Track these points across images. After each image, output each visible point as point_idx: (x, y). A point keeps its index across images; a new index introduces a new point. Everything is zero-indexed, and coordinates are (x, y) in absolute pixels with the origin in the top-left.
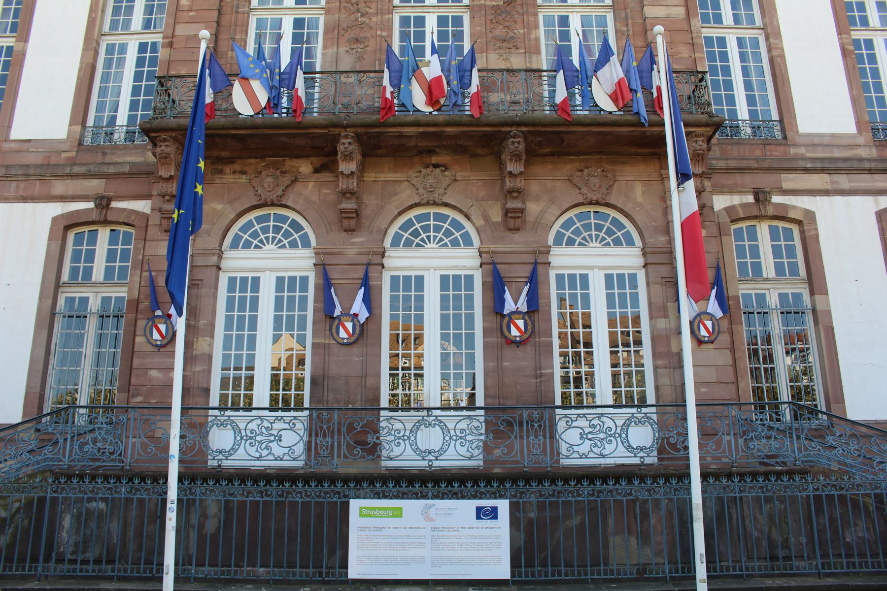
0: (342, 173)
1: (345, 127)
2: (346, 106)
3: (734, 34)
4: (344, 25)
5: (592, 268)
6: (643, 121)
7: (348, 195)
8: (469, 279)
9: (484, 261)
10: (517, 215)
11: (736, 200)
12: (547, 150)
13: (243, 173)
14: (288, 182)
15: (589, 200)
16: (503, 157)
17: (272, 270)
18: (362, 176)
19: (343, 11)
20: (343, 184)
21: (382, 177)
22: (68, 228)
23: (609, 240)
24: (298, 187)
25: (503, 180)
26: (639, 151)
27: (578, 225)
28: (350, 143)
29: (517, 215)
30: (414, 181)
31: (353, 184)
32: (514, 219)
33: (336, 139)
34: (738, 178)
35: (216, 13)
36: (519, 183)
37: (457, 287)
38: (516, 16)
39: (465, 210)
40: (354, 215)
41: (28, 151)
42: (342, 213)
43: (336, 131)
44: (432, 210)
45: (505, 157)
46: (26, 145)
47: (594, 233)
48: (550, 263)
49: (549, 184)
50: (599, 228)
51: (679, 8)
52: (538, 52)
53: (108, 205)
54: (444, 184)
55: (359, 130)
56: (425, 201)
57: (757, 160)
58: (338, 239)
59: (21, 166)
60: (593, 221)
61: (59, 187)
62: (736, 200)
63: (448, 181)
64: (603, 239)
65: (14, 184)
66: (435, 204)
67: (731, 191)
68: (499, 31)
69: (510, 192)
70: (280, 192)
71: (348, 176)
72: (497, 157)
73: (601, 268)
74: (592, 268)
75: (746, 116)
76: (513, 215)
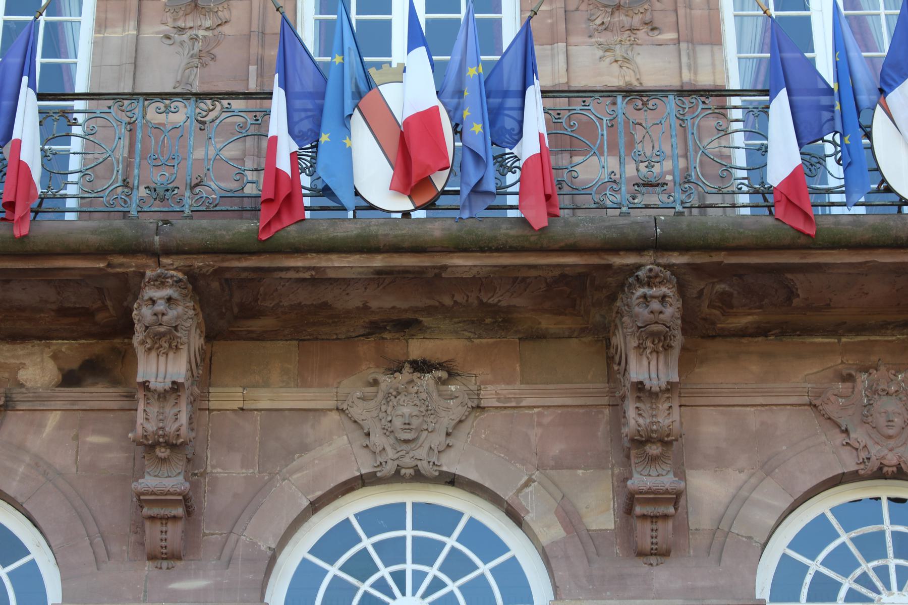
0: (145, 385)
1: (156, 254)
2: (160, 194)
7: (162, 452)
10: (661, 510)
12: (743, 321)
15: (874, 465)
16: (618, 340)
18: (205, 397)
20: (147, 419)
21: (265, 400)
25: (617, 407)
27: (844, 538)
28: (169, 300)
29: (661, 510)
30: (358, 411)
31: (177, 419)
32: (652, 525)
33: (128, 288)
36: (666, 417)
39: (507, 495)
43: (131, 264)
44: (409, 497)
45: (624, 340)
49: (753, 419)
52: (715, 39)
54: (447, 420)
55: (198, 262)
56: (390, 468)
60: (888, 527)
63: (456, 410)
66: (419, 477)
69: (640, 441)
71: (163, 396)
72: (601, 337)
76: (649, 510)
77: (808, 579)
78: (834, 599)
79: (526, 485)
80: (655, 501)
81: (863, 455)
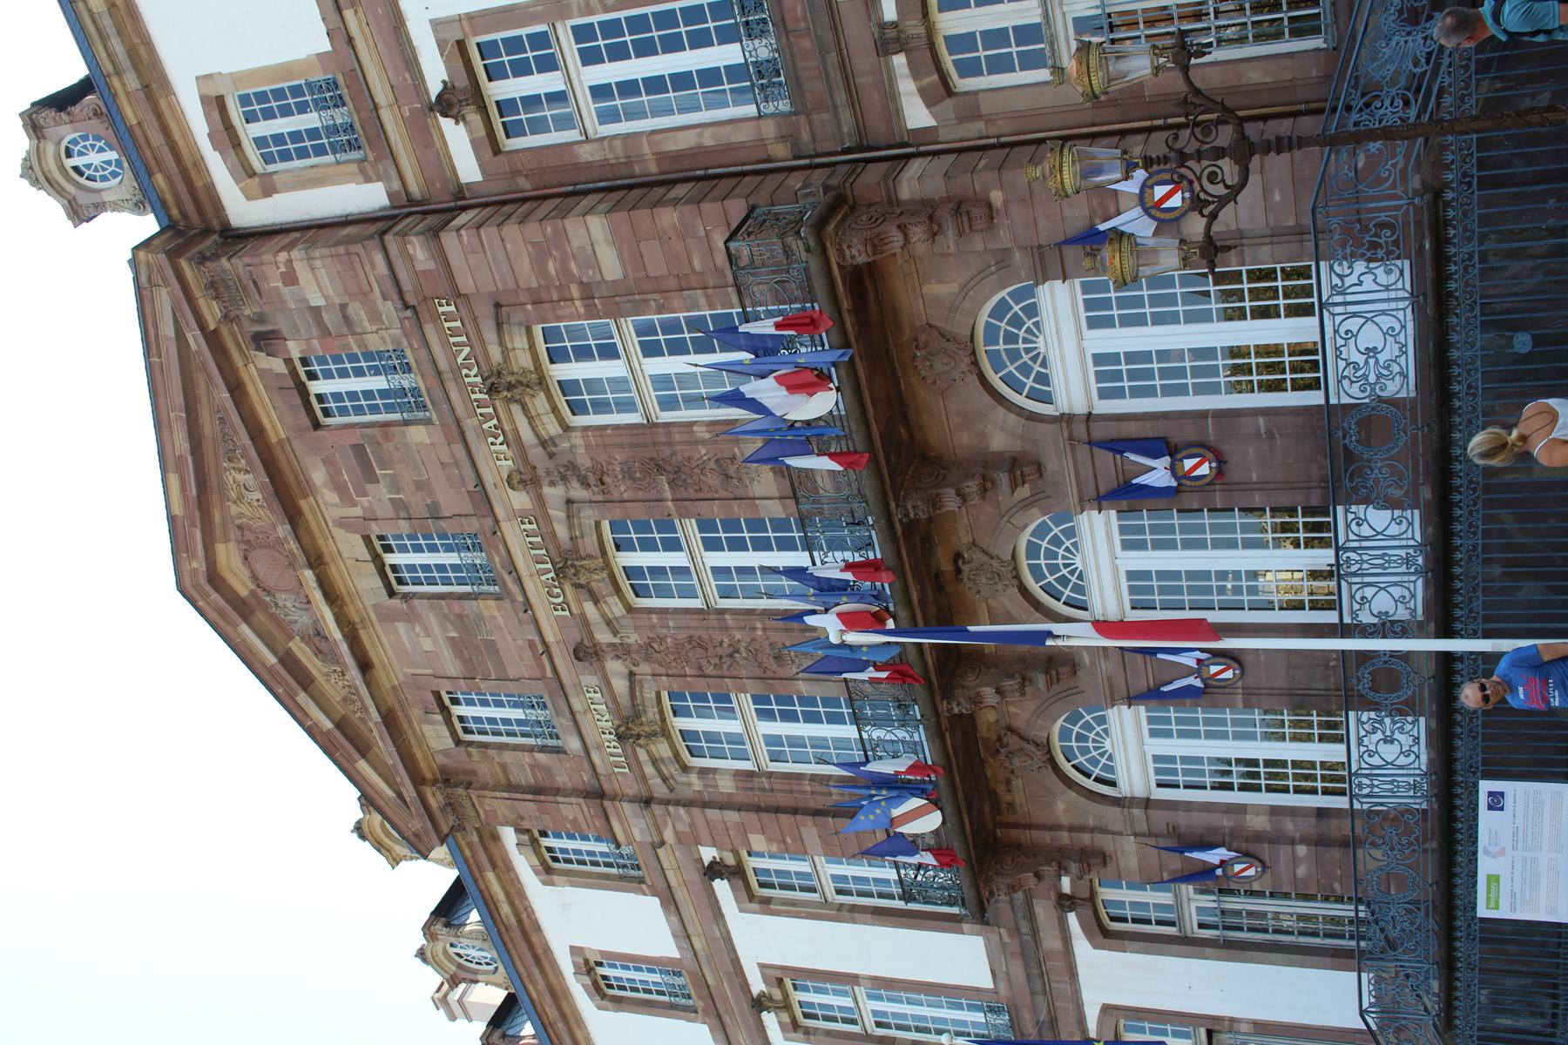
1: (937, 714)
3: (579, 74)
4: (758, 672)
5: (1082, 351)
6: (846, 359)
11: (907, 87)
12: (903, 431)
13: (1008, 782)
14: (1015, 738)
17: (1142, 743)
19: (735, 673)
22: (1106, 933)
24: (1018, 724)
26: (871, 296)
34: (864, 80)
35: (782, 816)
41: (1008, 973)
43: (945, 724)
46: (999, 975)
51: (591, 226)
54: (985, 559)
56: (1015, 582)
57: (823, 52)
59: (1029, 981)
61: (1051, 942)
62: (907, 87)
63: (978, 556)
65: (1054, 985)
67: (891, 97)
68: (713, 480)
70: (1031, 747)
74: (1082, 351)
75: (735, 48)
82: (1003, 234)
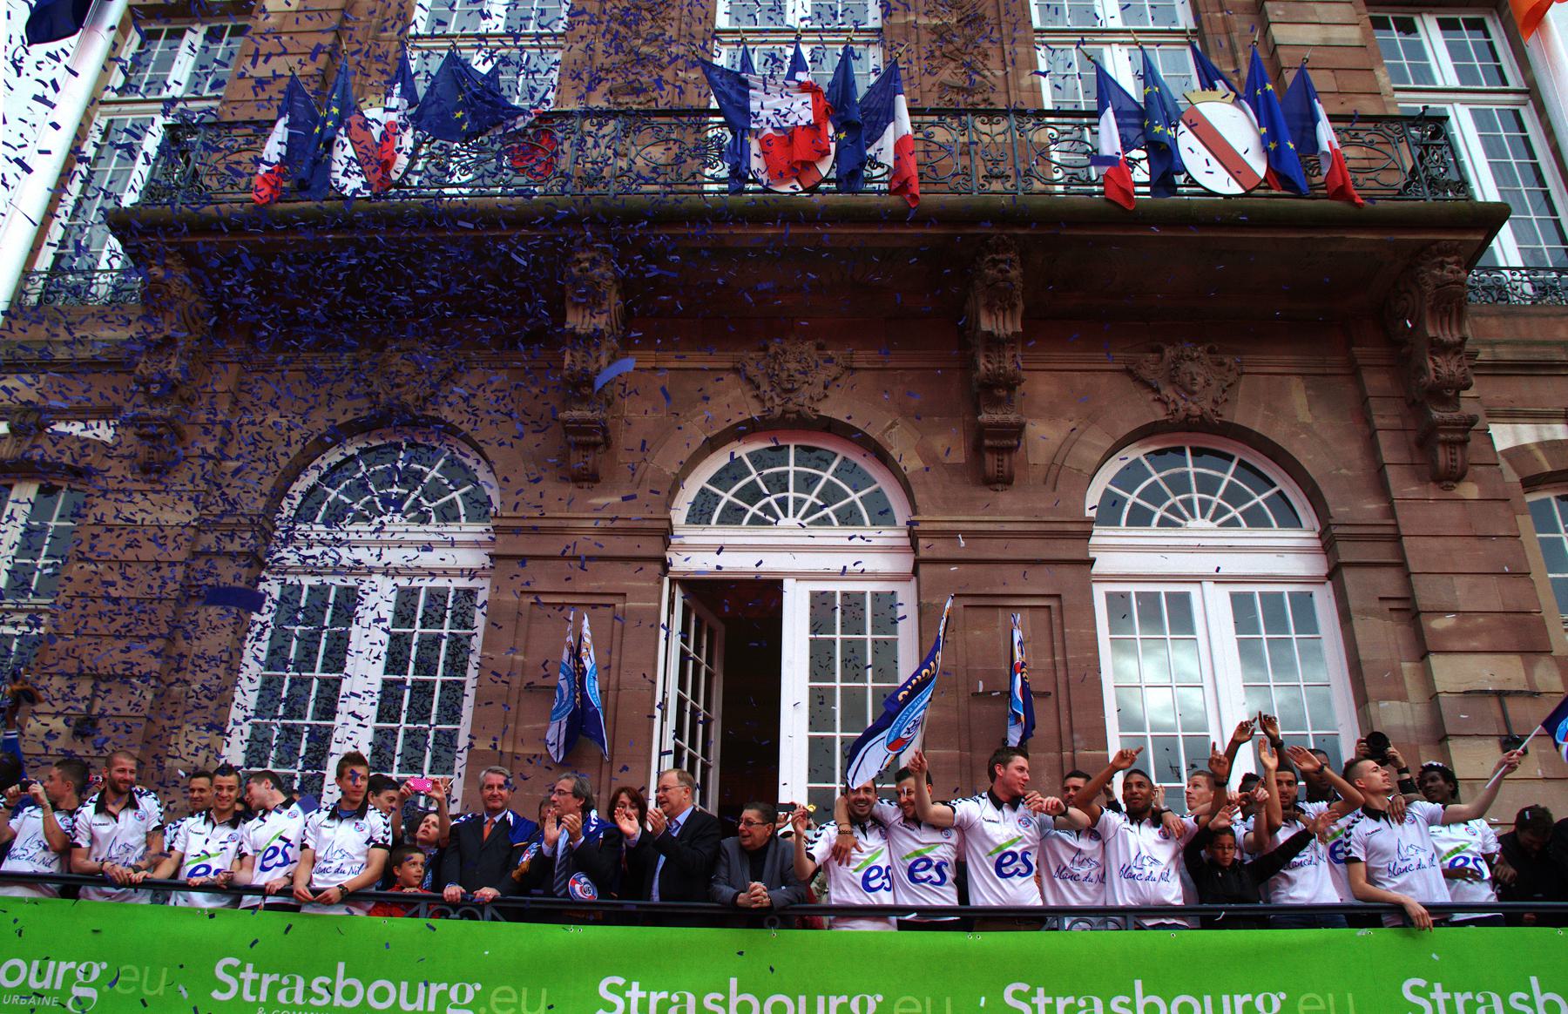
5: (1197, 580)
8: (886, 606)
9: (923, 554)
10: (1006, 442)
23: (1235, 512)
29: (1006, 442)
30: (751, 370)
37: (853, 621)
38: (986, 45)
40: (599, 438)
42: (568, 431)
47: (1196, 496)
48: (1092, 562)
49: (1080, 381)
50: (1208, 485)
53: (41, 427)
58: (555, 499)
64: (1221, 511)
73: (1220, 579)
74: (1197, 580)
76: (996, 443)
77: (1127, 508)
78: (1148, 524)
79: (891, 427)
80: (1002, 436)
81: (1172, 407)
82: (1413, 490)
